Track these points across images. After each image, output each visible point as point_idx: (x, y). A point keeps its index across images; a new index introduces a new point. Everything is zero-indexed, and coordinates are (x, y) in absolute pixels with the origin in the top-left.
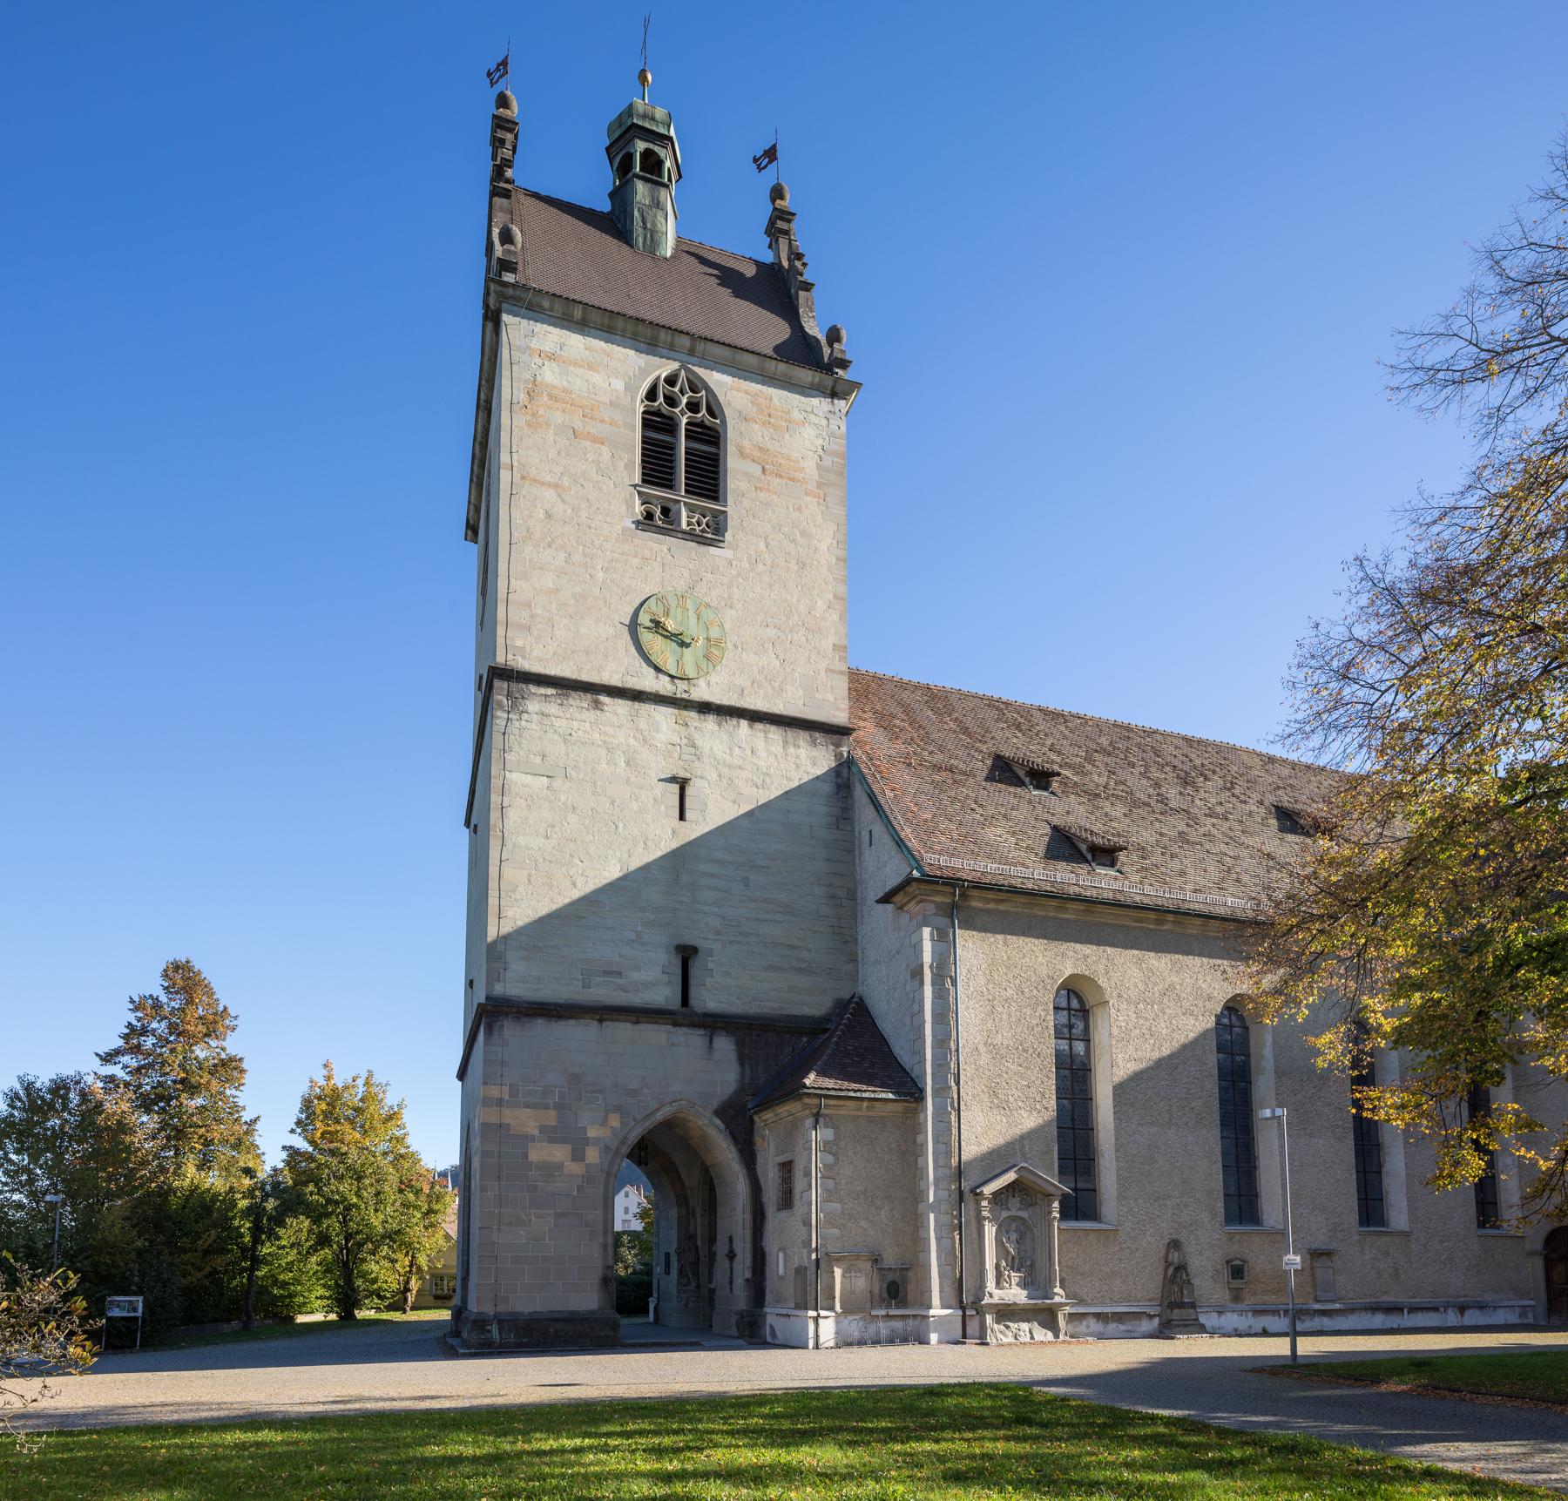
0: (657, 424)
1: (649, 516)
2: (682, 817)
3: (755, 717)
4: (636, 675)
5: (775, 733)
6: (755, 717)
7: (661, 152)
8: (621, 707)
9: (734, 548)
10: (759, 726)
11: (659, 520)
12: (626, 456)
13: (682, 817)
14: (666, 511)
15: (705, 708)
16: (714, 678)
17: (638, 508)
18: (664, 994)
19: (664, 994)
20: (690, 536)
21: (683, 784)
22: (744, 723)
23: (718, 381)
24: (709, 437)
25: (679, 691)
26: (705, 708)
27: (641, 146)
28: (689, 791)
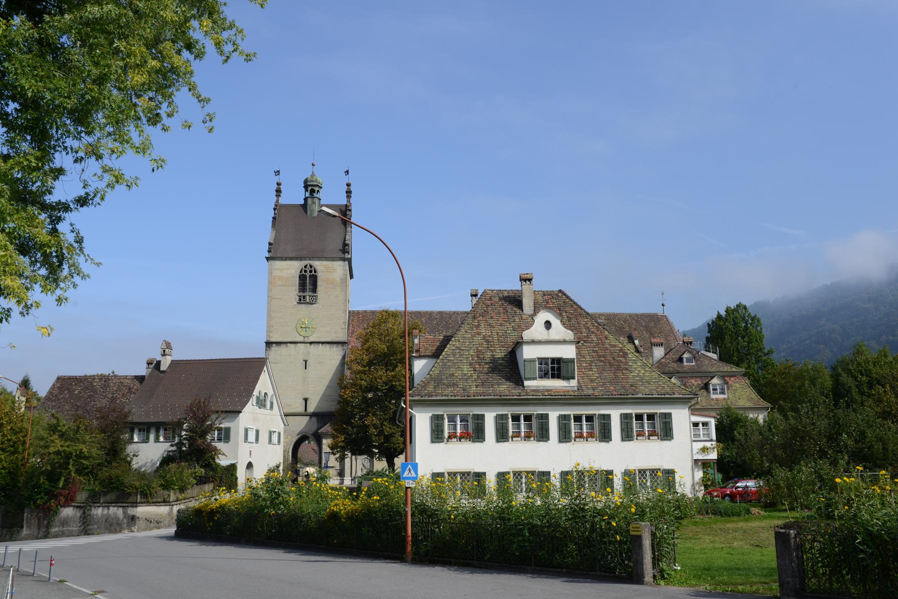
0: (302, 278)
1: (300, 300)
2: (306, 368)
3: (323, 343)
4: (295, 337)
5: (328, 346)
6: (323, 343)
7: (314, 188)
8: (293, 345)
9: (319, 303)
10: (324, 345)
11: (302, 300)
12: (295, 288)
13: (306, 368)
14: (304, 298)
15: (311, 343)
16: (314, 335)
17: (298, 298)
18: (301, 409)
19: (301, 409)
20: (308, 303)
21: (306, 362)
22: (320, 344)
23: (317, 264)
24: (314, 279)
25: (306, 340)
26: (311, 343)
27: (310, 188)
28: (307, 362)
